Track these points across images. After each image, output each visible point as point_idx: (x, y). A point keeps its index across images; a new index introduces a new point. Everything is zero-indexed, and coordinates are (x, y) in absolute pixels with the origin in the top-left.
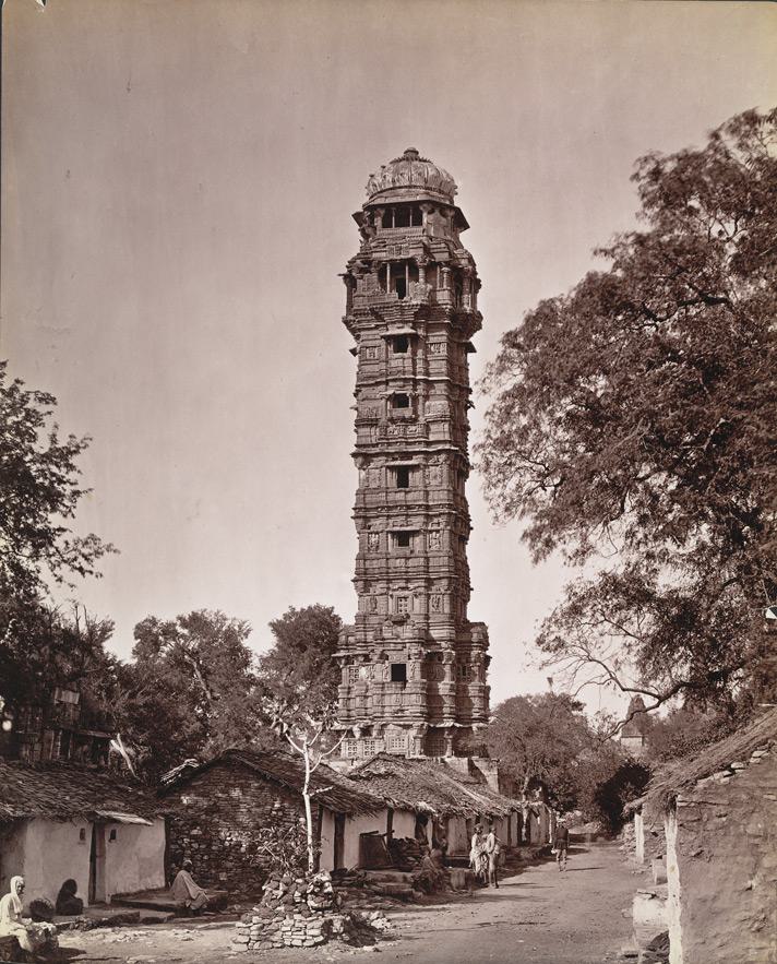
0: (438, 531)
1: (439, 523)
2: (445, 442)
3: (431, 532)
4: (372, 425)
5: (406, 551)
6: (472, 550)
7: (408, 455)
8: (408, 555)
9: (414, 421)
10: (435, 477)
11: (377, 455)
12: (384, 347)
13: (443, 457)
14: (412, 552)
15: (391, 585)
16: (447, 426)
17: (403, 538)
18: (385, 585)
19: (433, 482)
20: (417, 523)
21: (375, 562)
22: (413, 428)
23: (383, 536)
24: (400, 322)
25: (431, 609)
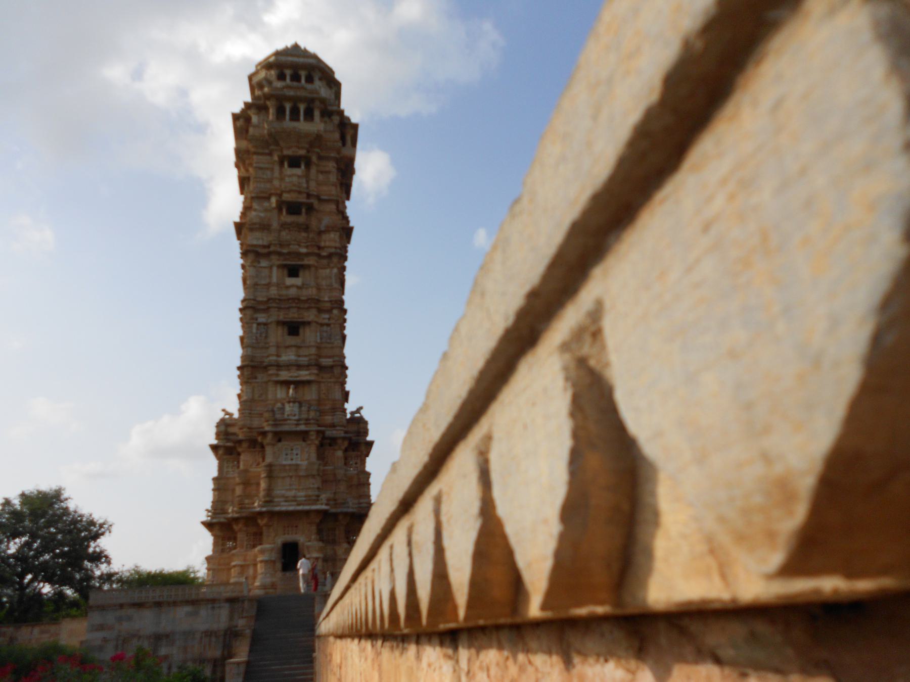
0: (328, 325)
1: (329, 319)
2: (336, 248)
3: (322, 325)
7: (299, 255)
9: (307, 228)
11: (268, 255)
12: (277, 168)
17: (293, 328)
19: (324, 283)
22: (304, 234)
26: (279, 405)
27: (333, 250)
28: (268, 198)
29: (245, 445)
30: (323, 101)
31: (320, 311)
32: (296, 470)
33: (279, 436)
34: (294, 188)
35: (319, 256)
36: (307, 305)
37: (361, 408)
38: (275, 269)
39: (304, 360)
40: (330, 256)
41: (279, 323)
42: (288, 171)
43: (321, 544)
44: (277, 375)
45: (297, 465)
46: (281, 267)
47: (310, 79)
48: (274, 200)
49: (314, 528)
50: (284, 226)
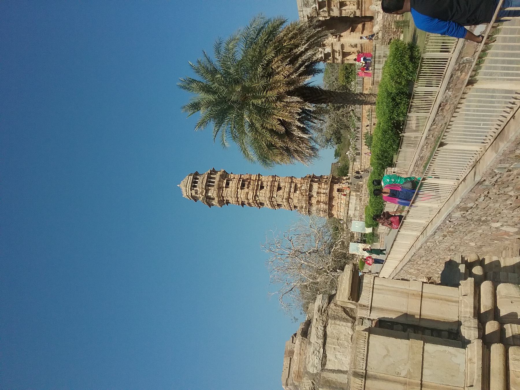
7: (258, 185)
9: (250, 182)
11: (256, 193)
17: (279, 188)
20: (276, 184)
28: (238, 192)
35: (259, 180)
39: (289, 186)
40: (259, 177)
46: (260, 190)
50: (248, 188)
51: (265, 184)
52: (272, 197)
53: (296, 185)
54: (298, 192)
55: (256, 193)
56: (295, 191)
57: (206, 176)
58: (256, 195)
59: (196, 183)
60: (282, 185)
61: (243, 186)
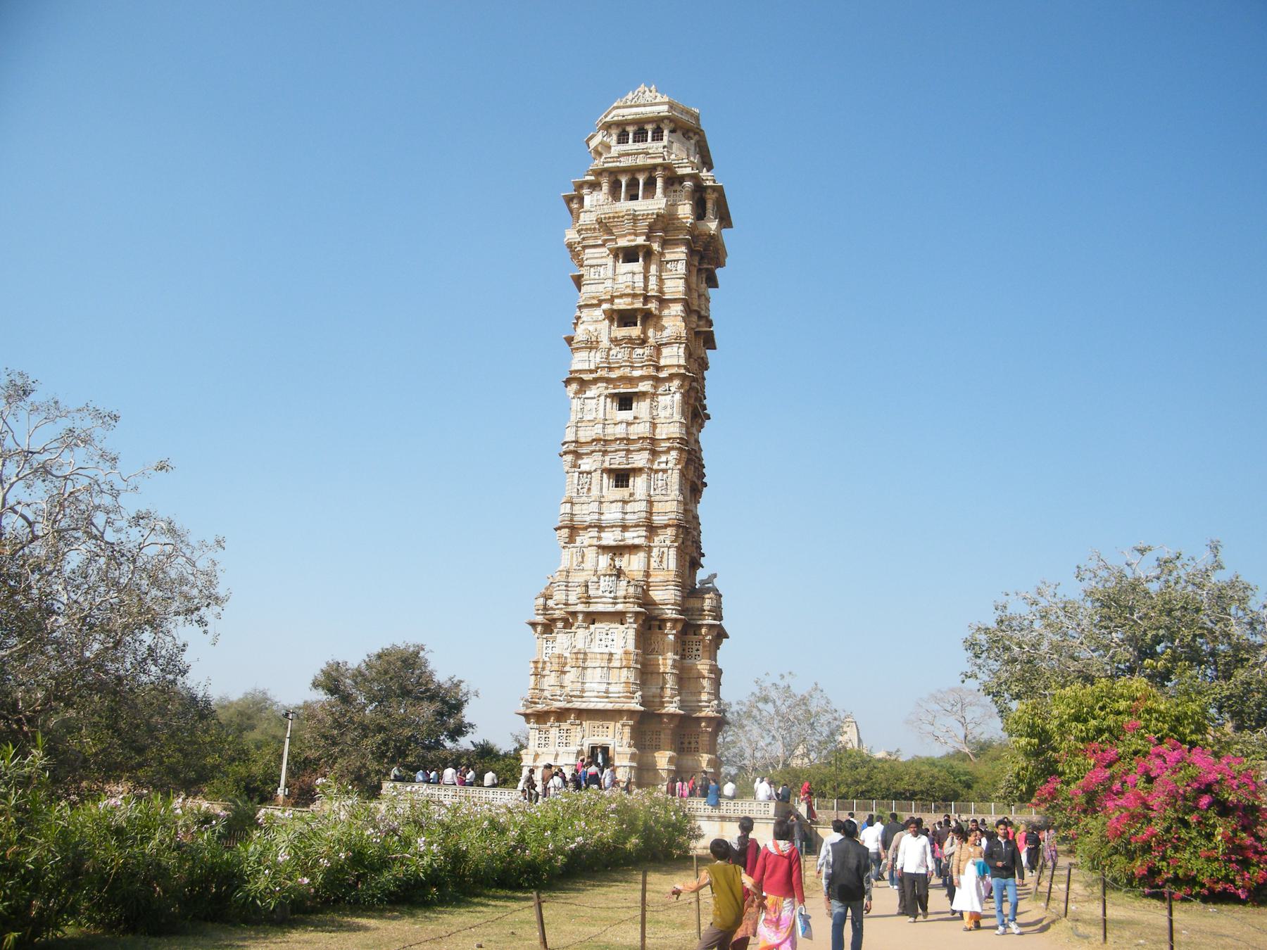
0: (665, 471)
2: (679, 366)
3: (657, 471)
4: (591, 348)
5: (623, 493)
6: (704, 509)
8: (626, 498)
9: (643, 342)
10: (665, 408)
11: (595, 381)
12: (610, 261)
13: (676, 383)
14: (632, 495)
15: (603, 535)
16: (682, 350)
17: (621, 477)
18: (596, 534)
20: (640, 460)
21: (585, 506)
22: (640, 351)
23: (596, 476)
24: (630, 234)
25: (653, 565)
26: (595, 579)
27: (674, 370)
28: (599, 305)
29: (560, 624)
30: (667, 167)
31: (654, 453)
32: (610, 660)
33: (592, 618)
34: (629, 291)
36: (639, 445)
37: (715, 576)
38: (602, 398)
40: (671, 377)
41: (604, 471)
42: (624, 267)
43: (634, 750)
44: (599, 538)
45: (611, 654)
47: (658, 135)
48: (605, 306)
49: (627, 730)
51: (641, 408)
52: (578, 455)
53: (634, 548)
54: (604, 560)
55: (595, 381)
56: (604, 549)
57: (660, 161)
58: (584, 384)
59: (640, 136)
60: (639, 485)
61: (625, 318)
